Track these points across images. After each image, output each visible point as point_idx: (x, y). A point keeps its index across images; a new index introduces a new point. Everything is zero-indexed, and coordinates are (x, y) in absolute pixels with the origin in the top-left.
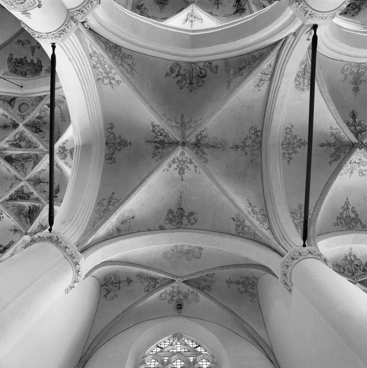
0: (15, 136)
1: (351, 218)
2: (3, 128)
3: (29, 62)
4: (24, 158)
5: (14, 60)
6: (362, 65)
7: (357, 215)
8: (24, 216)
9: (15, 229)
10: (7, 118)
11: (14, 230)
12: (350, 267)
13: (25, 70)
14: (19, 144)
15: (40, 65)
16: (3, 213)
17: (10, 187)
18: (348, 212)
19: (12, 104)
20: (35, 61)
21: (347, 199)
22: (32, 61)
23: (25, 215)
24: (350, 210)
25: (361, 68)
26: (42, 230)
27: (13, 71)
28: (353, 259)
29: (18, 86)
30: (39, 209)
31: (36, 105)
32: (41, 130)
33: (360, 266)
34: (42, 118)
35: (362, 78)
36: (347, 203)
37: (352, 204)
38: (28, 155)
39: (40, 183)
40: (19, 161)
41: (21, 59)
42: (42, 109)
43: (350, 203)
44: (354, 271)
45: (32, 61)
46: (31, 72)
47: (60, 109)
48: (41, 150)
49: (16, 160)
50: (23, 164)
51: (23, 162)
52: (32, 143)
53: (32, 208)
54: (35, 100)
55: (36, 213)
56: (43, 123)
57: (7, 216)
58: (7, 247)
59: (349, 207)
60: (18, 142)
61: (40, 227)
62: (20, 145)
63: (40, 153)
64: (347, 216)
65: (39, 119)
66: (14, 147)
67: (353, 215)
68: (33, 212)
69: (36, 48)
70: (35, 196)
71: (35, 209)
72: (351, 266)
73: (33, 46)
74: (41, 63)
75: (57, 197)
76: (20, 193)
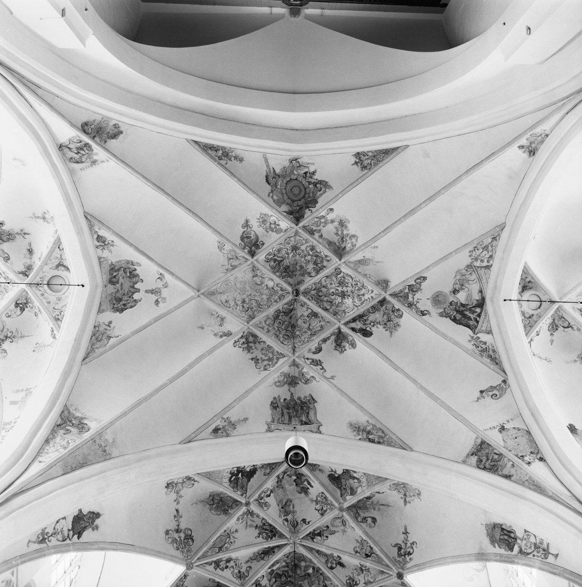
2: (29, 248)
3: (136, 286)
13: (121, 280)
15: (128, 305)
20: (136, 296)
22: (138, 290)
27: (114, 267)
29: (78, 285)
32: (24, 310)
41: (137, 276)
45: (138, 290)
60: (3, 275)
69: (157, 297)
73: (162, 292)
74: (131, 307)
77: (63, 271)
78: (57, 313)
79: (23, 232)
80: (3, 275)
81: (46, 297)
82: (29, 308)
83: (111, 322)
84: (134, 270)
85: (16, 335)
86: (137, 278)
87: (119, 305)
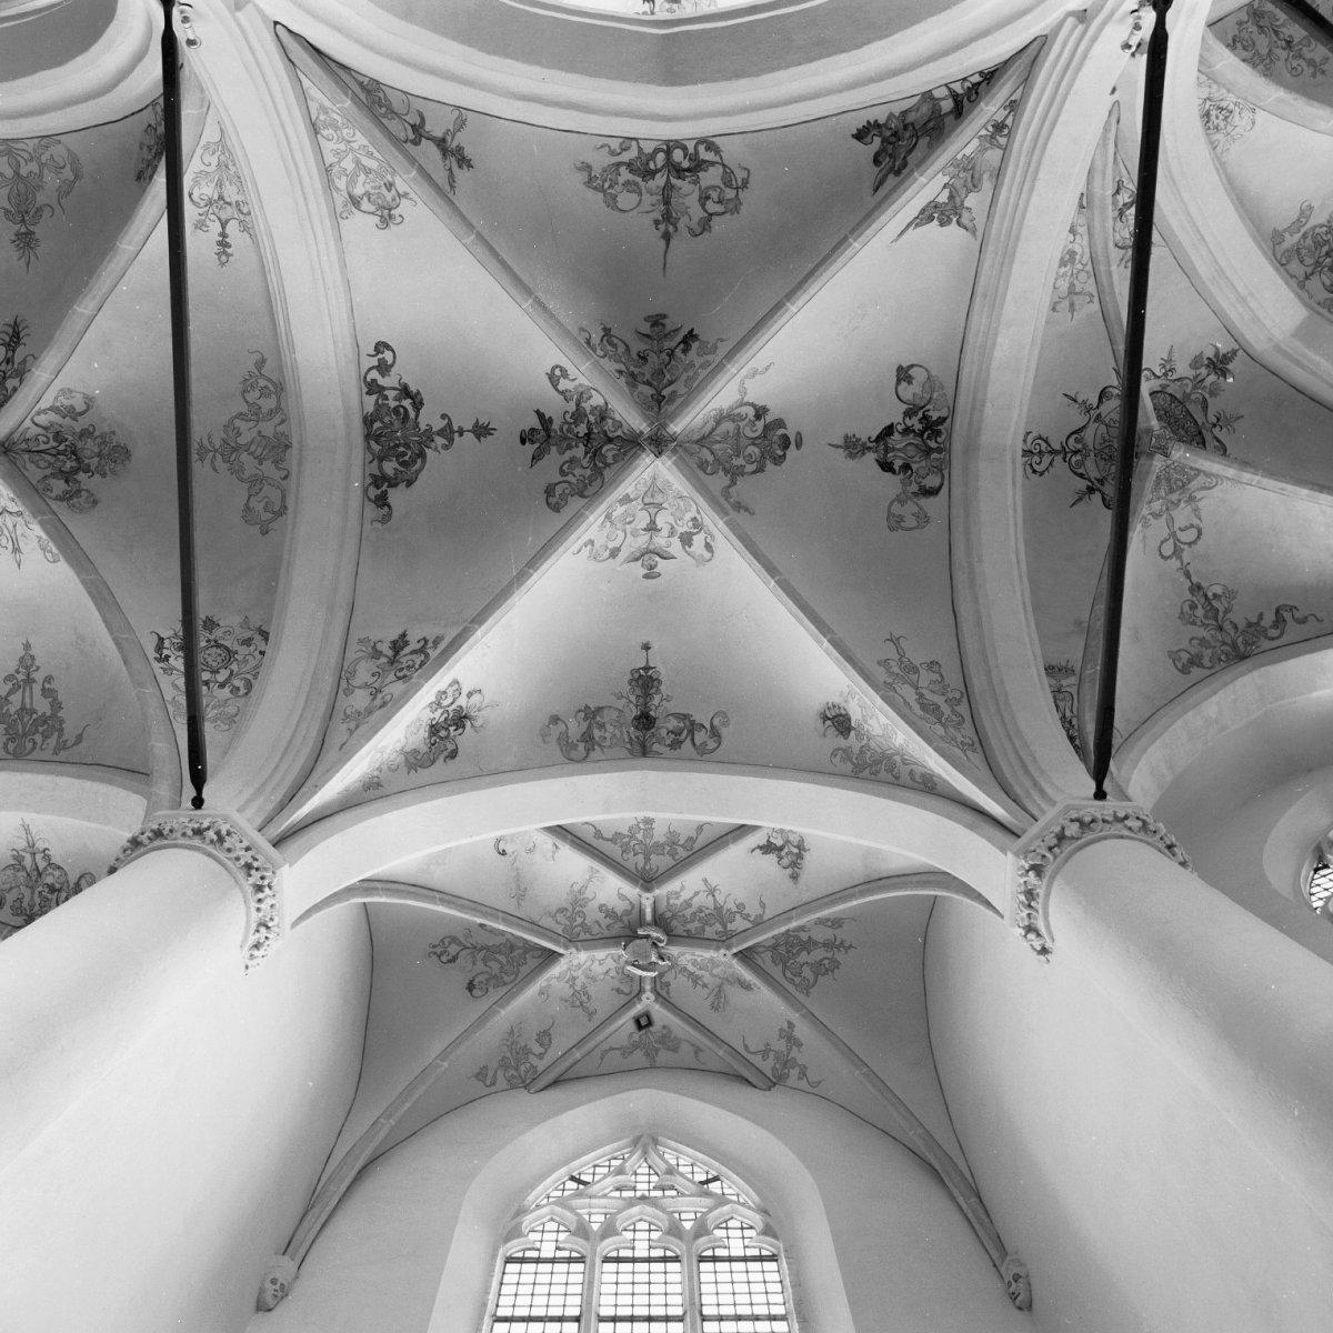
1: (35, 716)
6: (18, 146)
7: (56, 705)
12: (27, 893)
18: (27, 694)
21: (27, 646)
24: (37, 688)
25: (22, 163)
28: (42, 865)
33: (59, 890)
35: (41, 199)
36: (27, 662)
37: (45, 665)
43: (37, 663)
44: (37, 908)
59: (34, 675)
64: (23, 708)
67: (43, 706)
72: (33, 893)
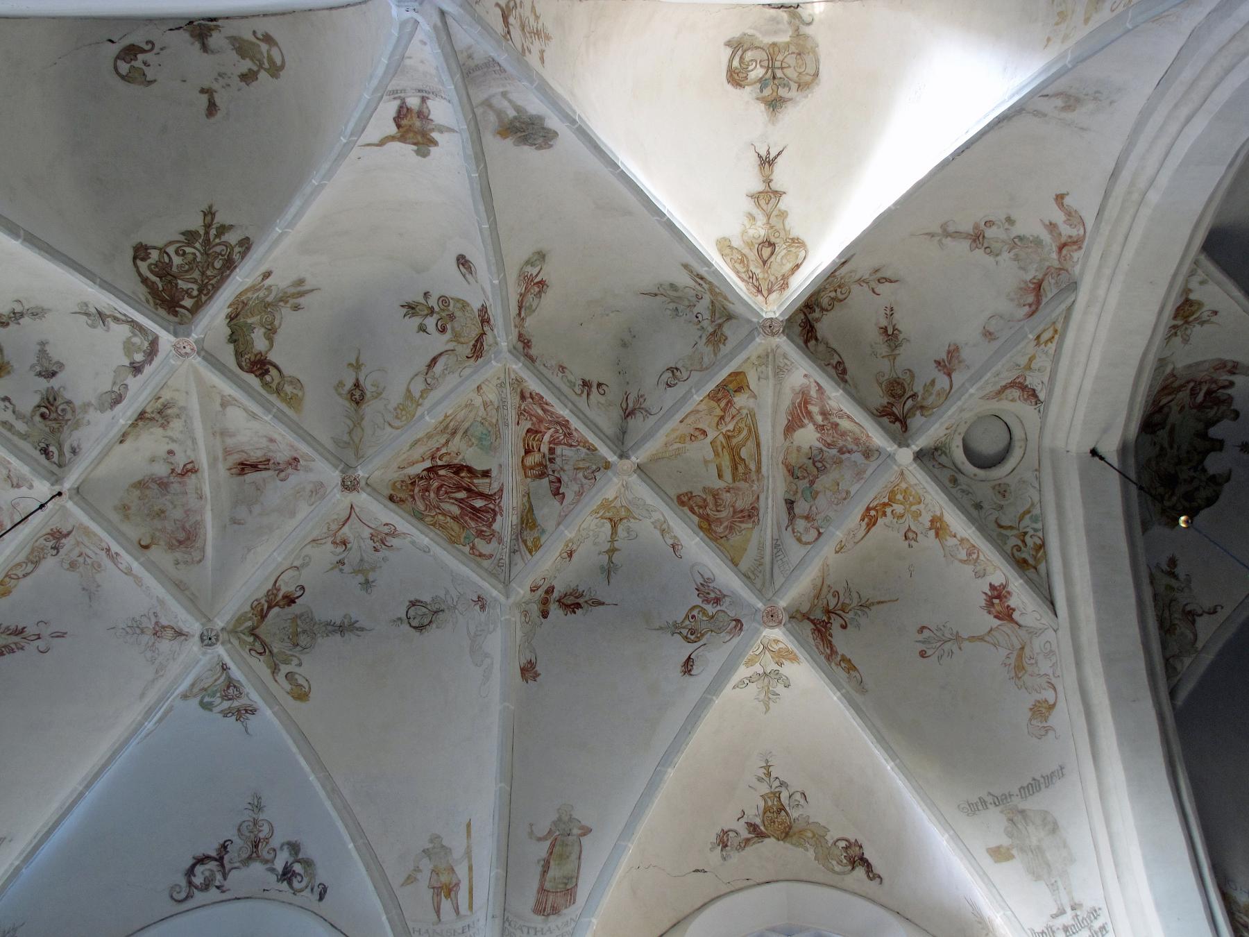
0: (848, 417)
2: (884, 323)
3: (1214, 432)
4: (734, 441)
5: (1225, 377)
8: (438, 449)
9: (363, 396)
10: (938, 363)
11: (357, 385)
14: (806, 421)
16: (448, 335)
17: (586, 384)
19: (1008, 391)
20: (1214, 464)
22: (1218, 445)
23: (444, 451)
26: (371, 531)
30: (480, 534)
31: (1005, 523)
32: (874, 524)
34: (937, 535)
38: (753, 466)
39: (611, 520)
40: (722, 418)
42: (982, 557)
45: (1218, 445)
46: (1162, 452)
47: (981, 639)
48: (777, 546)
49: (724, 410)
50: (704, 433)
51: (712, 434)
52: (812, 483)
53: (481, 484)
54: (1028, 512)
55: (455, 510)
56: (909, 529)
57: (434, 361)
58: (267, 372)
61: (386, 530)
62: (803, 426)
63: (761, 547)
65: (932, 521)
66: (793, 403)
68: (459, 488)
70: (546, 510)
71: (479, 503)
74: (1210, 502)
75: (545, 614)
76: (557, 431)
77: (1013, 400)
78: (1014, 541)
79: (879, 275)
80: (819, 419)
81: (964, 487)
82: (889, 519)
83: (1173, 562)
84: (1224, 387)
85: (847, 601)
86: (1223, 408)
87: (1174, 499)
